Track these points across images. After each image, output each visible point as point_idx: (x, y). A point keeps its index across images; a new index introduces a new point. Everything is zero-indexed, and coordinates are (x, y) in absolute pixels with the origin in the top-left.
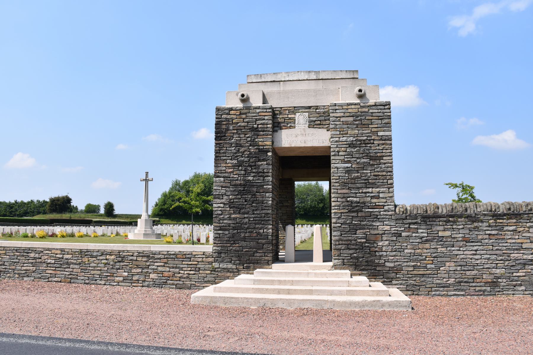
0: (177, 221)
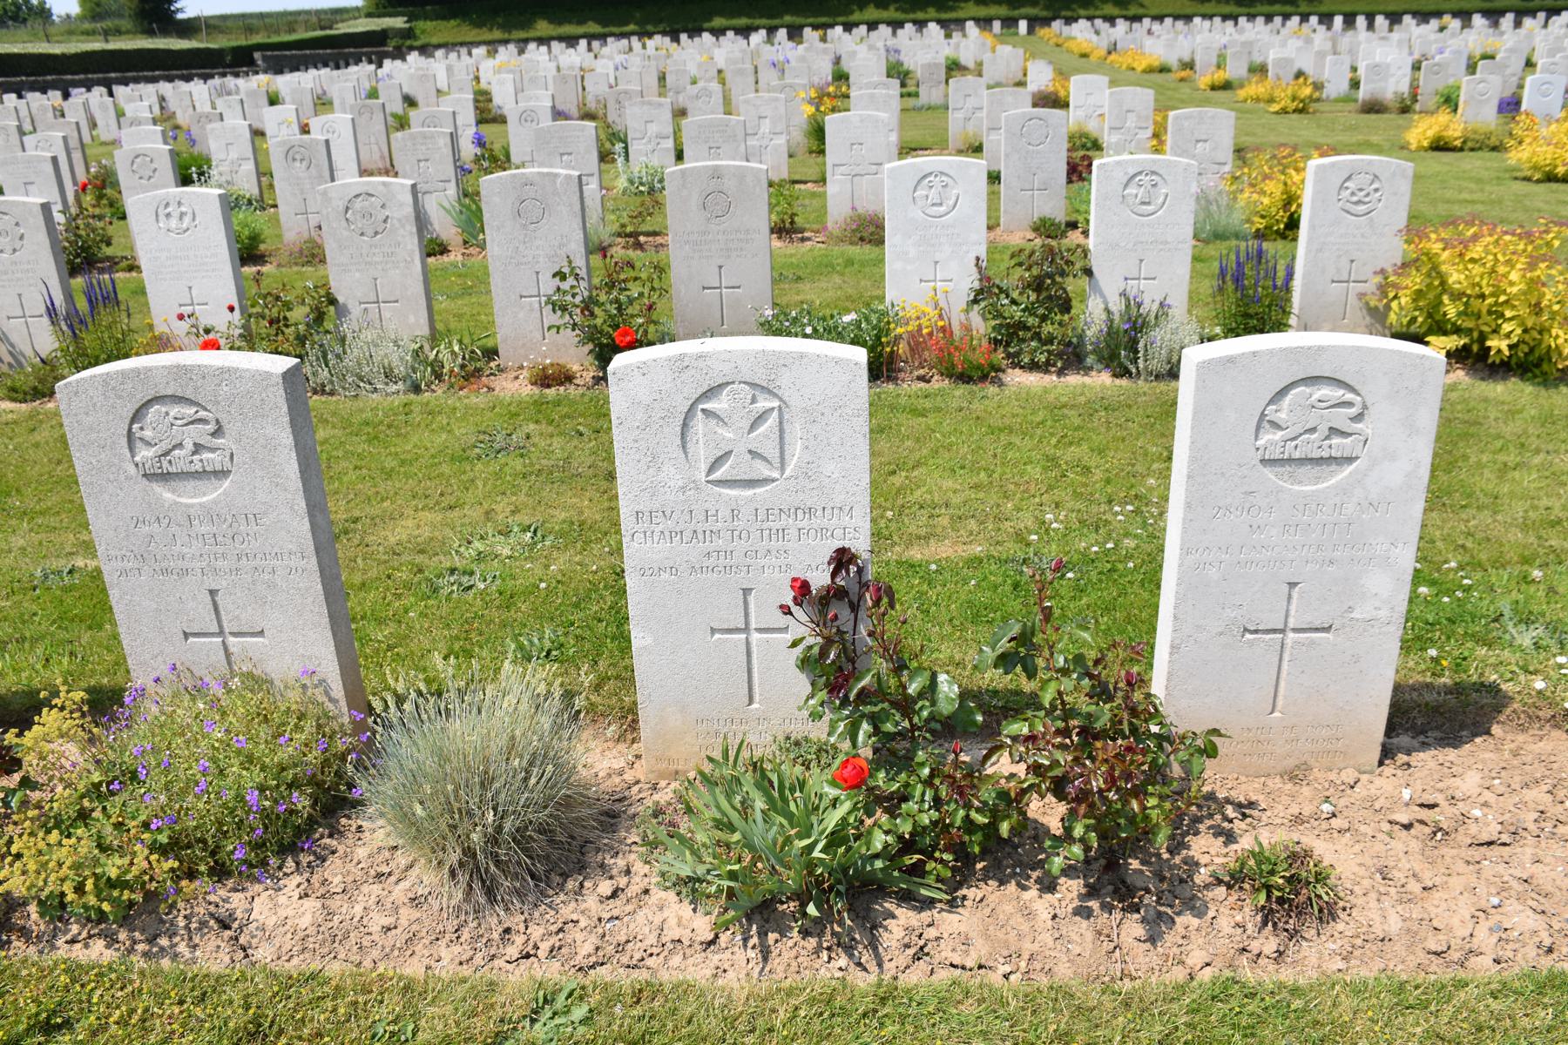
0: (507, 27)
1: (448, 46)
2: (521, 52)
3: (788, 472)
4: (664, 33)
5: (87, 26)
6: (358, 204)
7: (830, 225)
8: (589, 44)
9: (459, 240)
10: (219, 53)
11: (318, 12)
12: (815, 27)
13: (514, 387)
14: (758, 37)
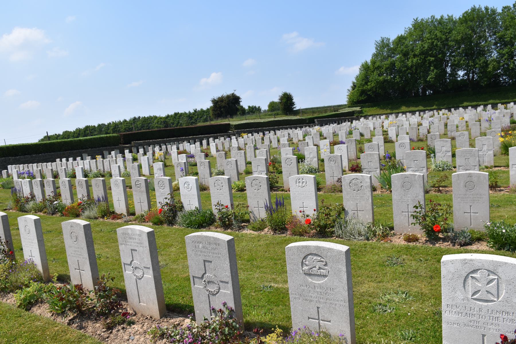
0: (392, 109)
1: (373, 116)
2: (397, 117)
3: (500, 299)
4: (446, 109)
5: (270, 113)
6: (353, 182)
7: (511, 185)
8: (419, 113)
9: (380, 187)
10: (305, 120)
11: (334, 106)
12: (502, 104)
13: (399, 241)
14: (480, 109)
